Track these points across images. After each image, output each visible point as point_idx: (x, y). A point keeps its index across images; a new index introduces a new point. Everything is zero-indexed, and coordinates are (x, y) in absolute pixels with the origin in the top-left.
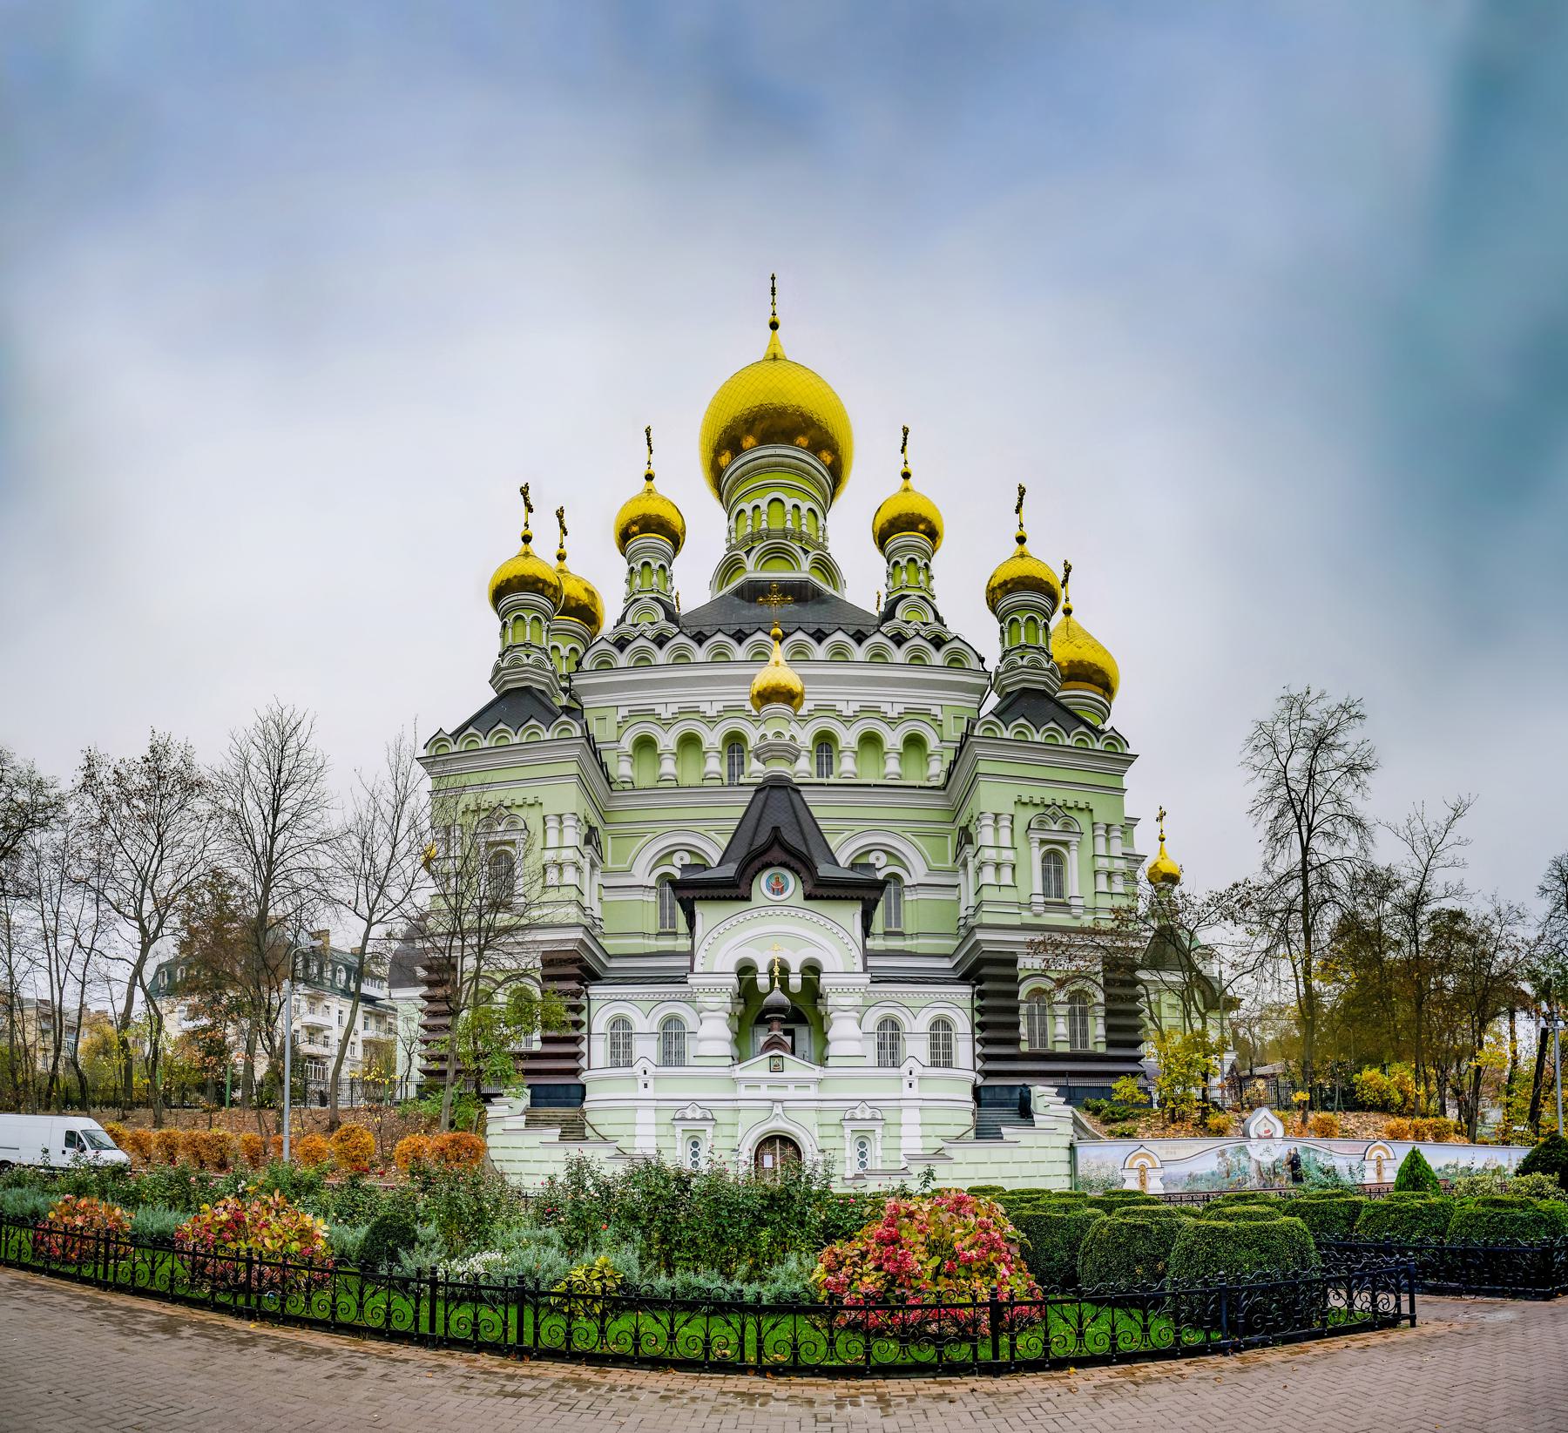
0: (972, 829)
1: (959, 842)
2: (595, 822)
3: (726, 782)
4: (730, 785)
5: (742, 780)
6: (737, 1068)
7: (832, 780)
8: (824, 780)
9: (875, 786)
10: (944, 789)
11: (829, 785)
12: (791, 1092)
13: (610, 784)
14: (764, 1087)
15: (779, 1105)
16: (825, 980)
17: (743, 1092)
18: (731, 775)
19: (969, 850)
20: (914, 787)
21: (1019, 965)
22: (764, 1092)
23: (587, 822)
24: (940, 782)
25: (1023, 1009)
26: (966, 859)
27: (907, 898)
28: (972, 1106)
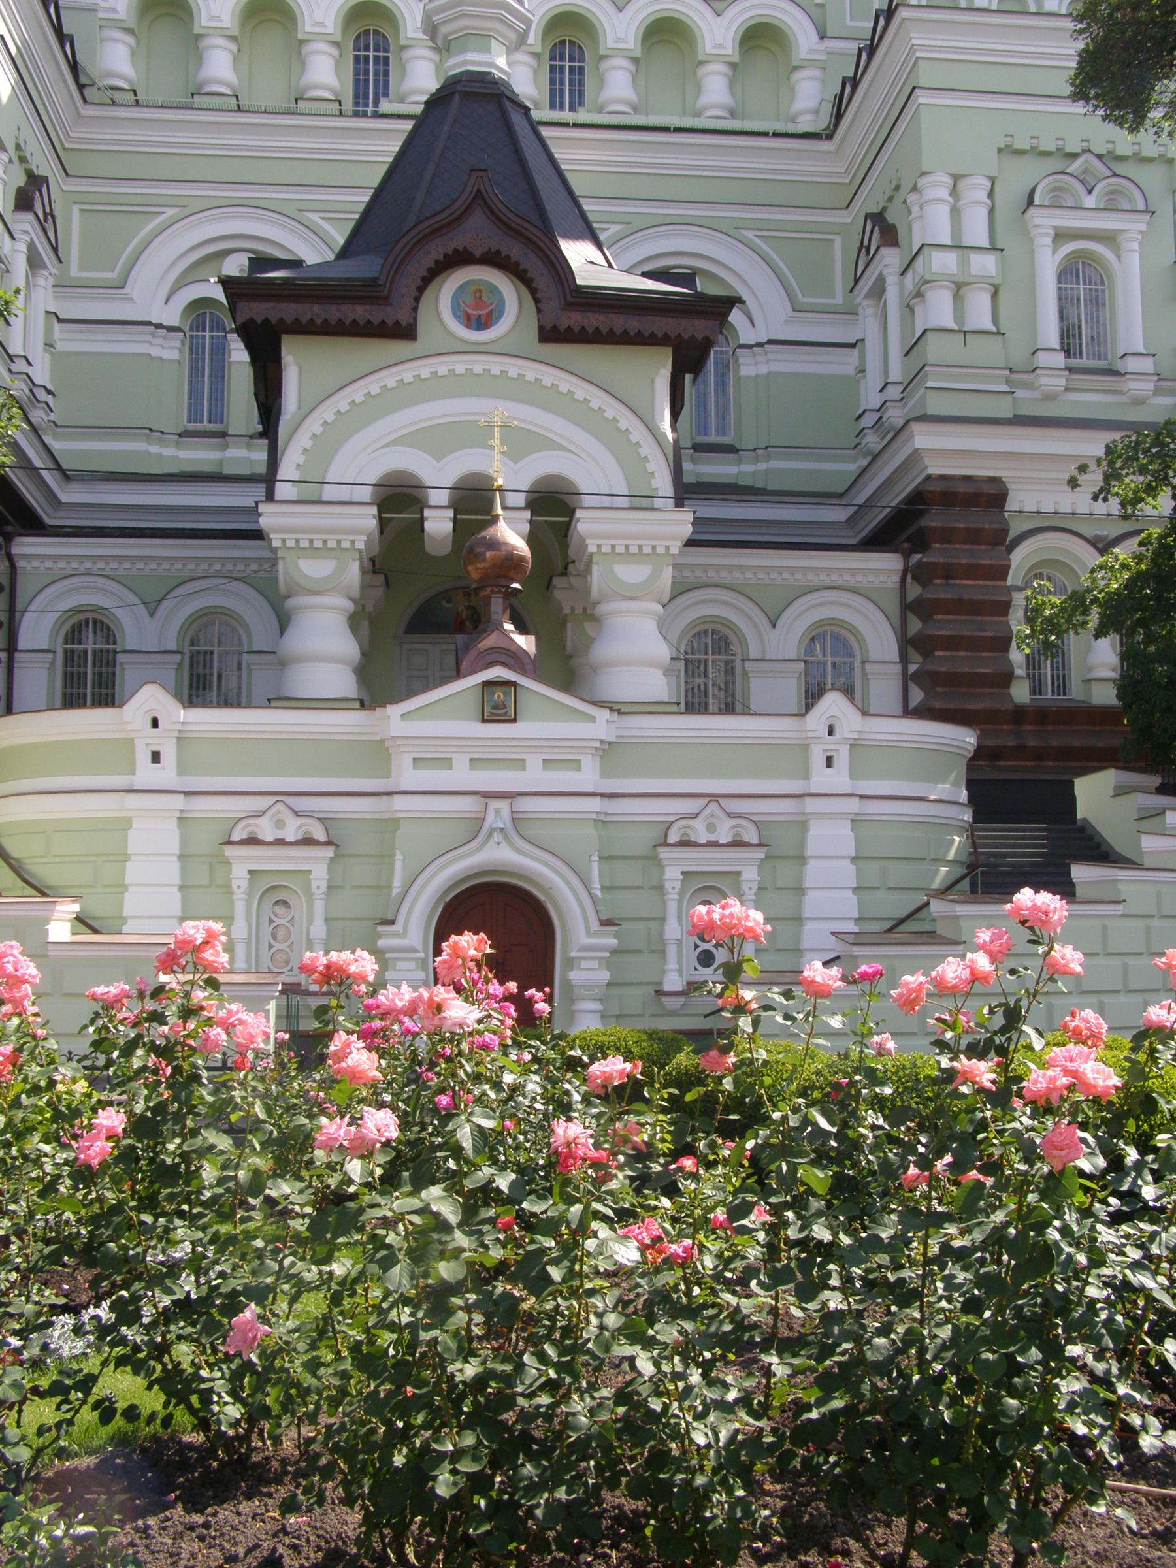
0: (891, 218)
1: (864, 248)
2: (44, 165)
3: (348, 106)
4: (356, 114)
5: (385, 106)
6: (394, 711)
7: (582, 116)
8: (566, 116)
9: (678, 130)
10: (830, 137)
11: (577, 126)
12: (533, 776)
13: (81, 87)
14: (461, 762)
15: (503, 805)
16: (586, 524)
17: (408, 776)
18: (360, 96)
19: (889, 260)
20: (764, 134)
21: (1012, 504)
22: (462, 776)
23: (23, 160)
24: (821, 123)
25: (1019, 599)
26: (881, 280)
27: (744, 371)
28: (967, 816)
